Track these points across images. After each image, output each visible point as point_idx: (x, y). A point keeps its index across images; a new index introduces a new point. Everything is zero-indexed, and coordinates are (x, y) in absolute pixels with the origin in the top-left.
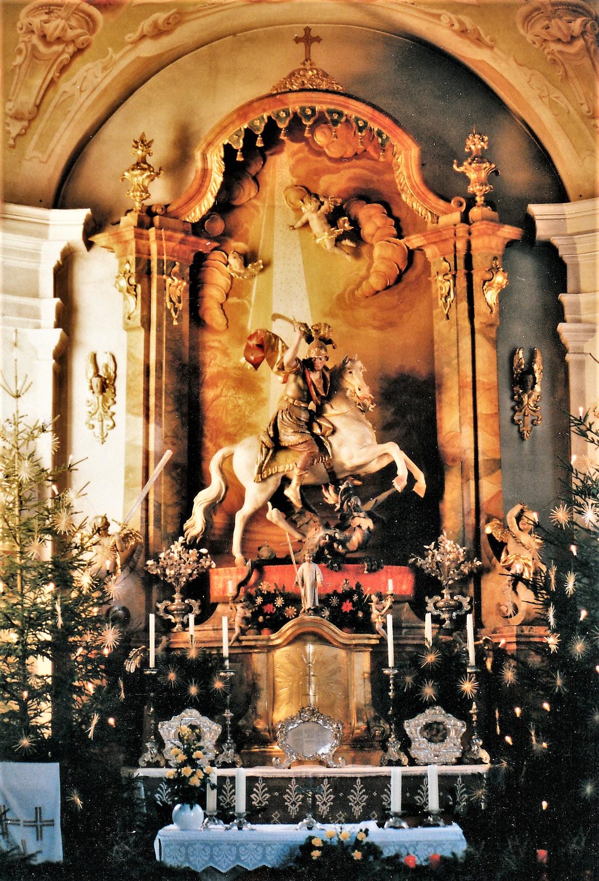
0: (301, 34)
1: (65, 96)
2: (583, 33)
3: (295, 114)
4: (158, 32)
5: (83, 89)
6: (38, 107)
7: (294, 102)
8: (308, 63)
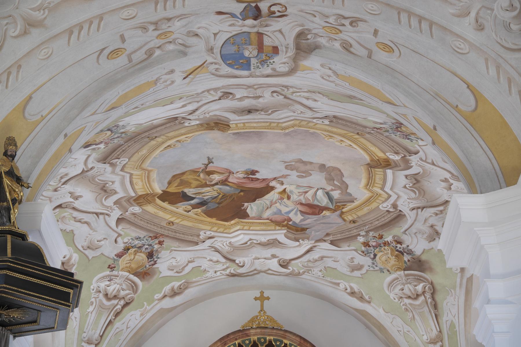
0: (258, 295)
1: (118, 330)
2: (424, 293)
3: (254, 342)
4: (174, 294)
5: (128, 327)
6: (101, 336)
7: (254, 335)
8: (262, 313)
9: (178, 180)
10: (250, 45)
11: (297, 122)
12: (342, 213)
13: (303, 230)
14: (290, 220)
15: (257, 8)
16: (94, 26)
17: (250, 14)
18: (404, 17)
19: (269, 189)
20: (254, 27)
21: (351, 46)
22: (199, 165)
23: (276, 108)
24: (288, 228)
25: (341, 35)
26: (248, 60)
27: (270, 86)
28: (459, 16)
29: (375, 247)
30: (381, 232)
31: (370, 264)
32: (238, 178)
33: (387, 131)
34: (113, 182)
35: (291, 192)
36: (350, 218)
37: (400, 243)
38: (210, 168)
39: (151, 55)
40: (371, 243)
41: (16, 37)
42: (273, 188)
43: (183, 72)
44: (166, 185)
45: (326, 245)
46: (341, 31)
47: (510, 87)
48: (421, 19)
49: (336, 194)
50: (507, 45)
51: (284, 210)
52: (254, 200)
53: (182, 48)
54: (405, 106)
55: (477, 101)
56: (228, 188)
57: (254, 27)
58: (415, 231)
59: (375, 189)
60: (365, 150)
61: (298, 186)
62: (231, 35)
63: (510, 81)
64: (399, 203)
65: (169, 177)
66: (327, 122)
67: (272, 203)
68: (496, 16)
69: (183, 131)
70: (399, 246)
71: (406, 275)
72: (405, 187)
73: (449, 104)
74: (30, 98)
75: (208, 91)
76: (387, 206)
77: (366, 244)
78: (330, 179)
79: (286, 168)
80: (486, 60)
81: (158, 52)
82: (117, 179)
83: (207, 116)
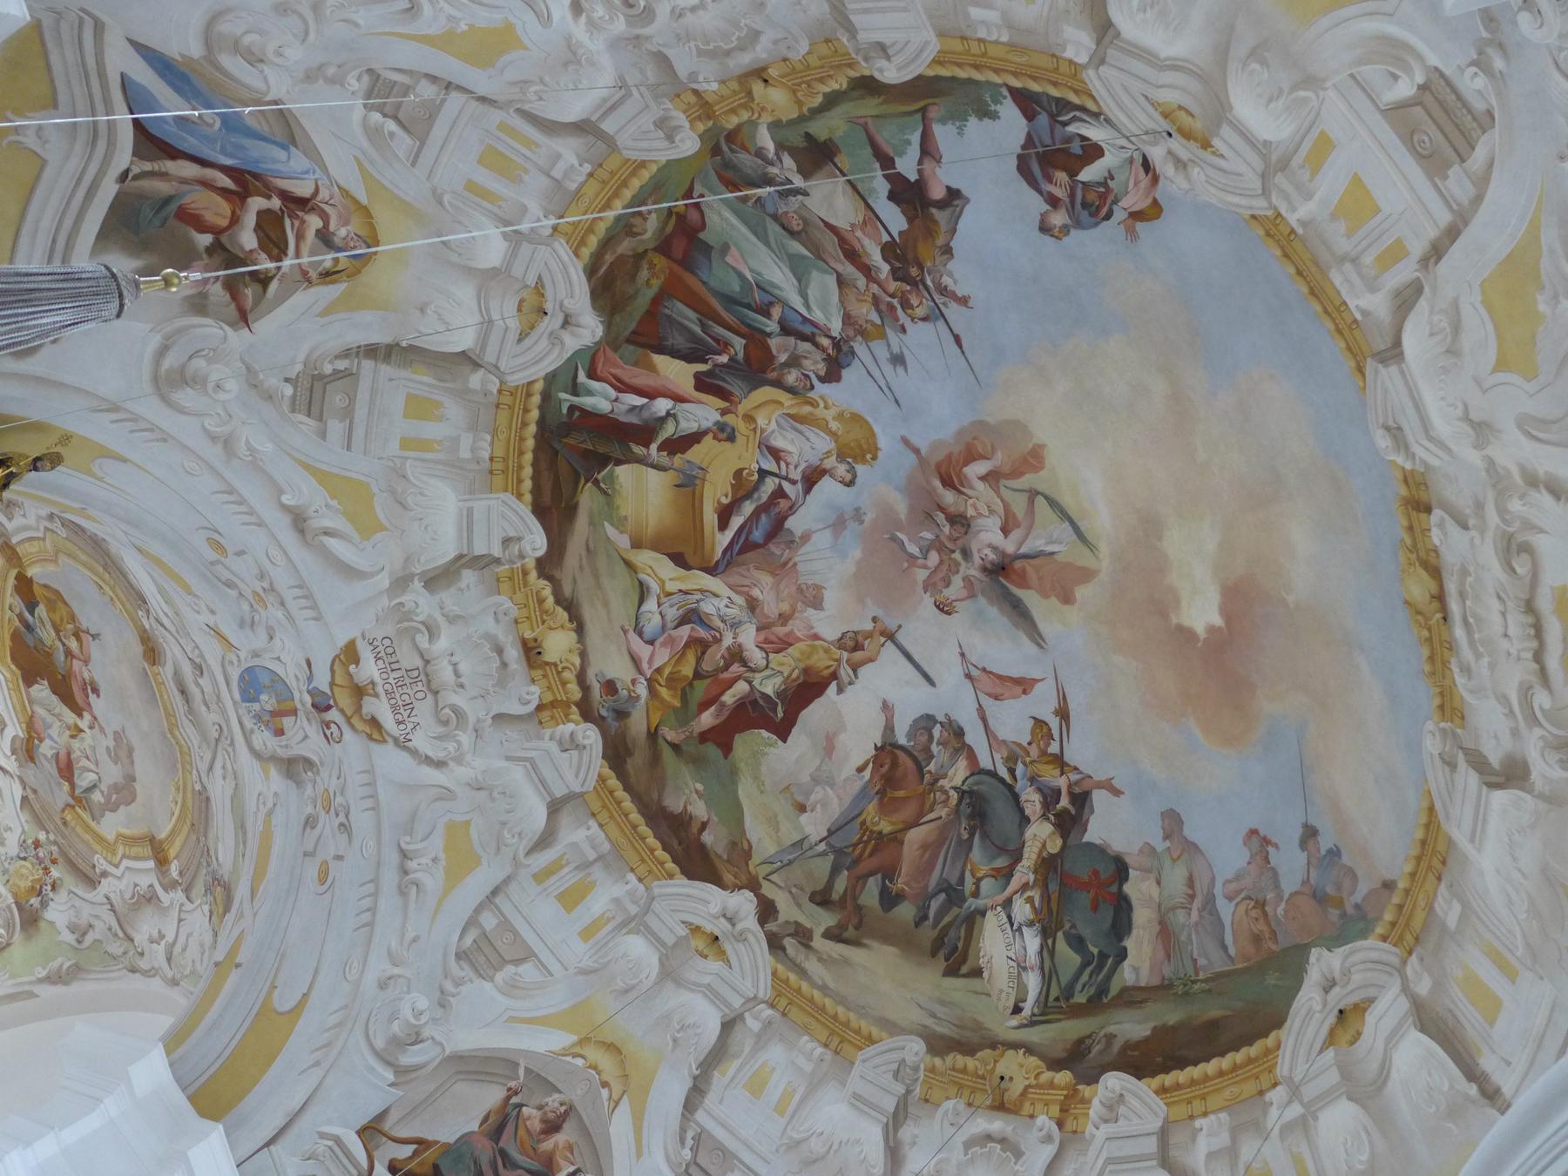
9: (53, 597)
10: (278, 702)
11: (186, 749)
12: (73, 807)
13: (32, 759)
14: (41, 741)
15: (329, 708)
16: (247, 518)
17: (318, 699)
18: (370, 888)
19: (79, 712)
20: (303, 704)
21: (313, 828)
22: (84, 625)
23: (197, 723)
24: (28, 740)
25: (323, 813)
26: (255, 699)
27: (227, 721)
28: (390, 954)
29: (37, 857)
30: (61, 860)
31: (10, 855)
32: (81, 672)
33: (209, 865)
34: (24, 516)
35: (83, 740)
36: (69, 818)
37: (54, 888)
38: (86, 638)
39: (229, 586)
40: (39, 849)
41: (203, 426)
42: (80, 715)
43: (216, 624)
44: (42, 582)
45: (18, 792)
46: (328, 812)
47: (317, 1050)
48: (372, 910)
49: (97, 797)
50: (372, 1020)
51: (54, 732)
52: (54, 692)
53: (248, 620)
54: (255, 915)
55: (290, 1012)
56: (62, 658)
57: (303, 704)
58: (77, 904)
59: (121, 847)
60: (173, 833)
61: (93, 748)
62: (282, 674)
63: (328, 1045)
64: (110, 879)
65: (55, 586)
66: (198, 787)
67: (58, 716)
68: (401, 999)
69: (128, 606)
70: (49, 888)
71: (9, 907)
72: (136, 885)
73: (276, 975)
74: (125, 460)
75: (197, 647)
76: (101, 863)
77: (37, 844)
78: (116, 788)
79: (116, 733)
80: (346, 1007)
81: (234, 593)
82: (31, 521)
83: (161, 640)
